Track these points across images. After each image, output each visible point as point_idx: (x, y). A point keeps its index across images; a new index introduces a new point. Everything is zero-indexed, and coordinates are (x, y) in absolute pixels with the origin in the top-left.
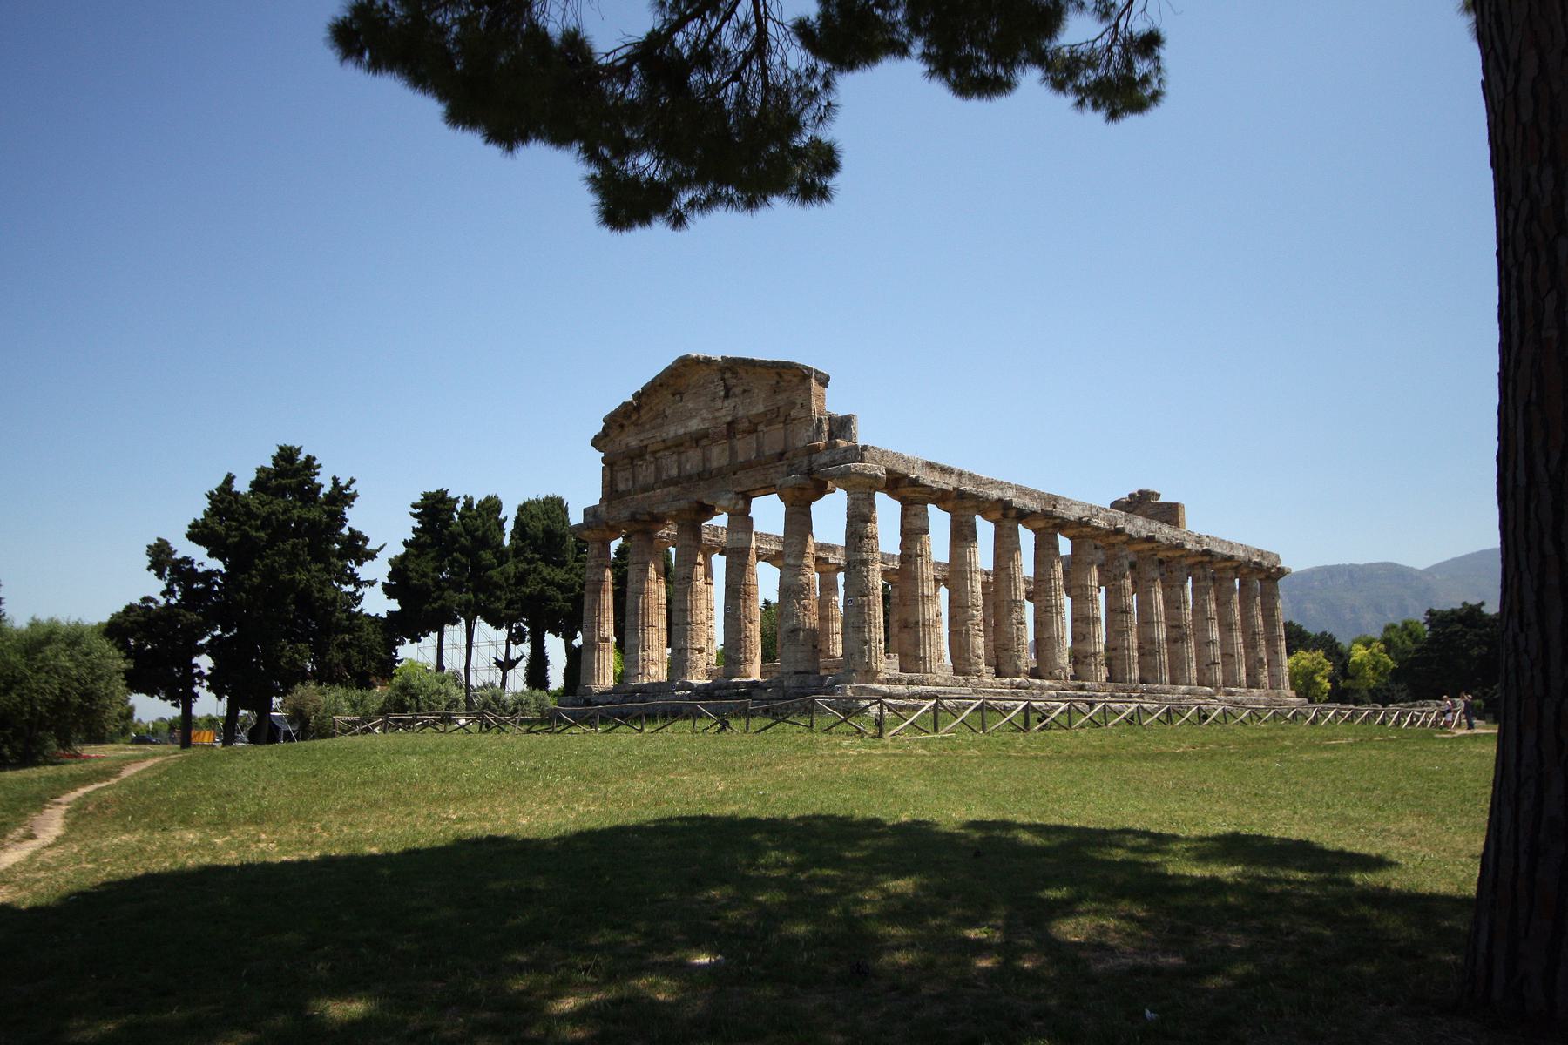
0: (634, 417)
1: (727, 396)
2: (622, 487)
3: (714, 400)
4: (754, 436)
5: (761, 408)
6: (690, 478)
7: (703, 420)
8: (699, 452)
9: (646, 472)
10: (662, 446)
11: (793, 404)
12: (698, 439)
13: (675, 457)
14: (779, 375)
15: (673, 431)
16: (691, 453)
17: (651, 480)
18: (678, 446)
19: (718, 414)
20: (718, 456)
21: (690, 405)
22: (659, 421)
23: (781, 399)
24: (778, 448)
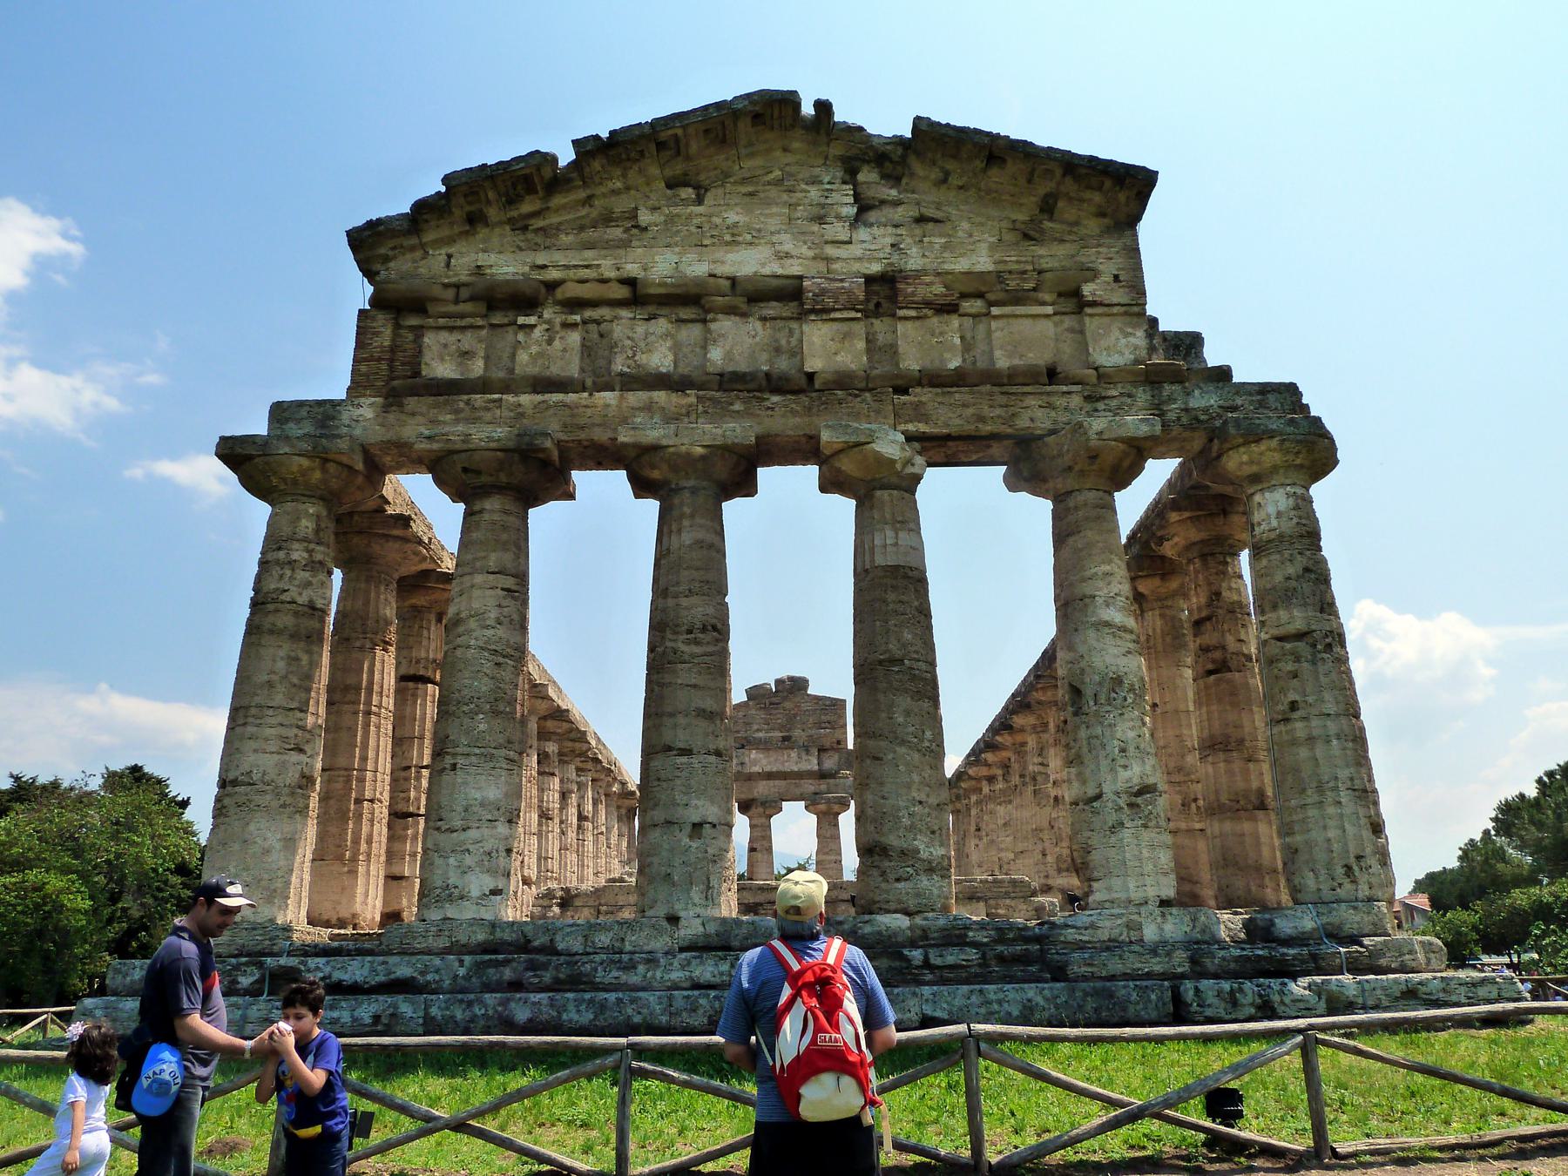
0: (527, 207)
1: (857, 221)
2: (443, 369)
3: (820, 220)
4: (955, 321)
5: (982, 261)
6: (731, 382)
7: (784, 256)
8: (755, 325)
9: (548, 345)
10: (622, 292)
11: (1093, 274)
12: (753, 296)
13: (662, 325)
14: (1047, 207)
15: (662, 265)
16: (724, 324)
17: (572, 368)
18: (689, 301)
19: (831, 251)
20: (825, 347)
21: (733, 217)
22: (616, 233)
23: (1052, 256)
24: (1038, 358)
